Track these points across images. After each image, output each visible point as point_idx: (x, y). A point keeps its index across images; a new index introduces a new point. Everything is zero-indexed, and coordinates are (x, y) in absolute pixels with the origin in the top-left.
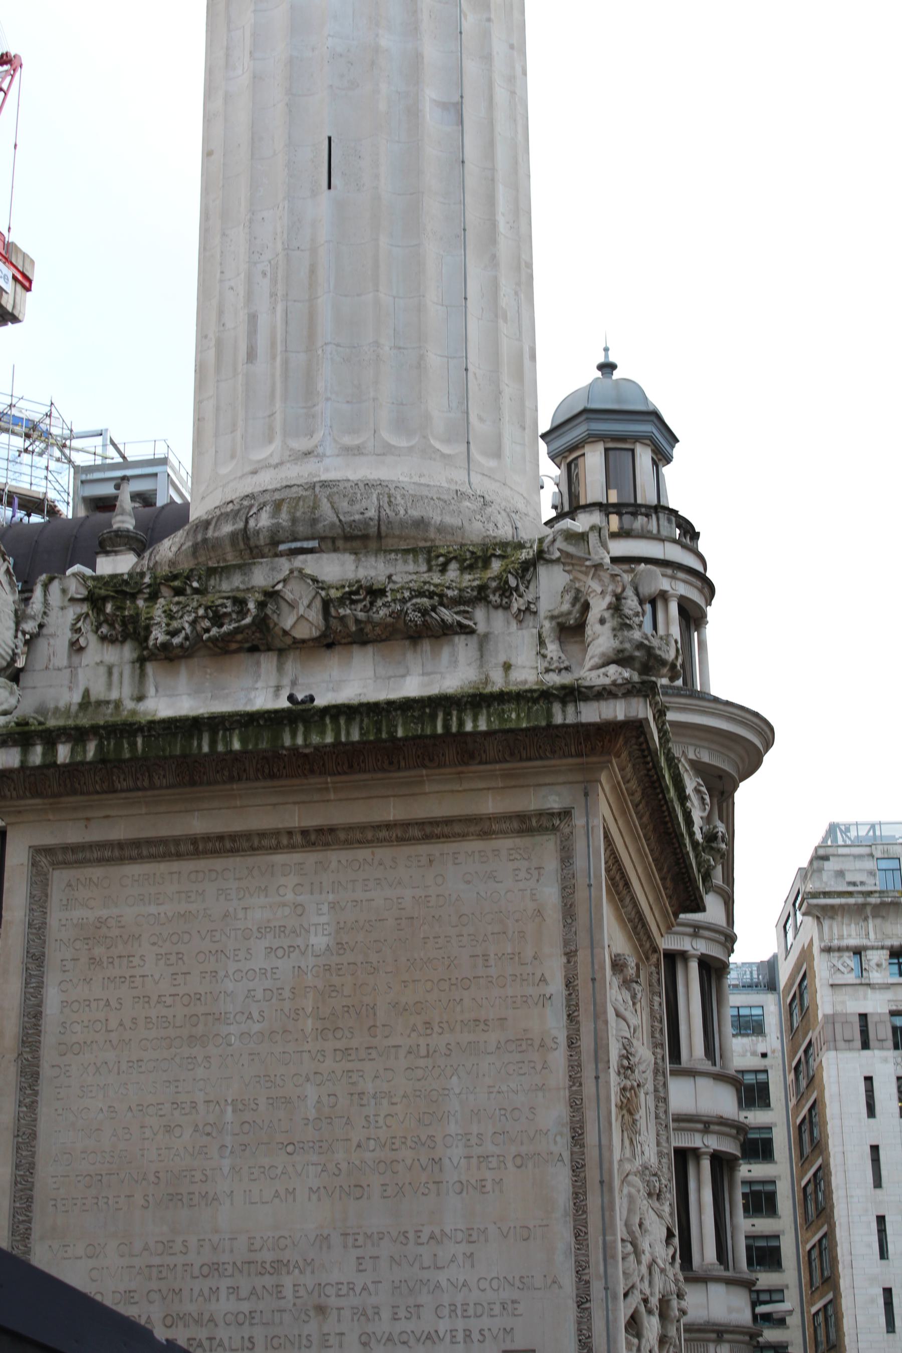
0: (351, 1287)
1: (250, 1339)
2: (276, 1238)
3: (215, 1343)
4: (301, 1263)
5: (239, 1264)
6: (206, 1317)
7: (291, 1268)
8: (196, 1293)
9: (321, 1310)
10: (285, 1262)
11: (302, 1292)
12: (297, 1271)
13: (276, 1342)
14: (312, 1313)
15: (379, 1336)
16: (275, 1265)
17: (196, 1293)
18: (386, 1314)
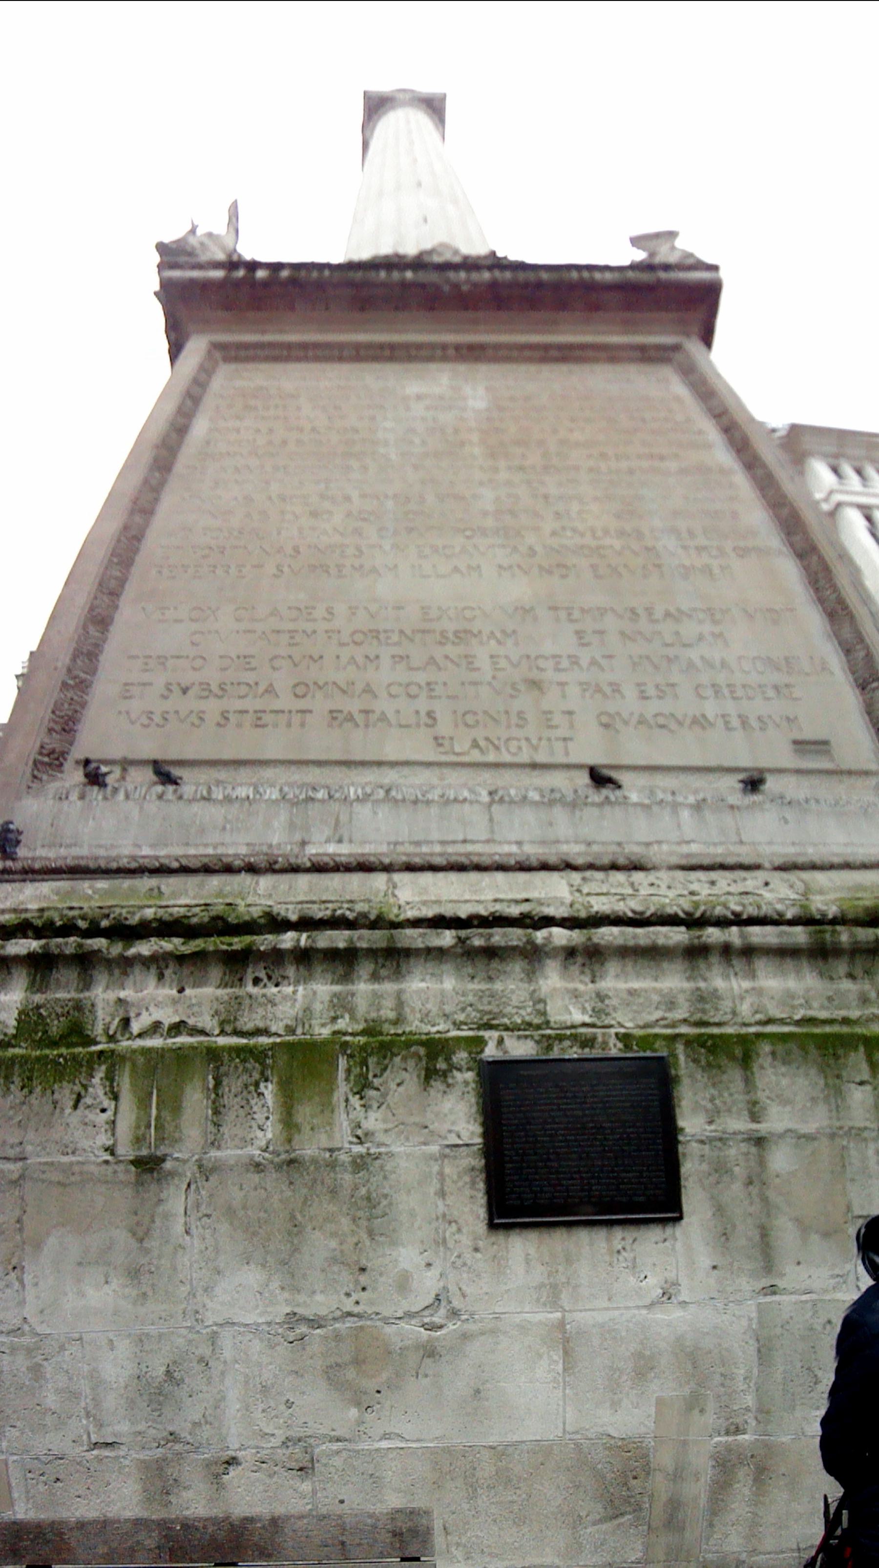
0: (574, 661)
1: (430, 714)
3: (373, 717)
4: (498, 635)
5: (408, 632)
6: (359, 686)
7: (485, 639)
8: (344, 660)
9: (535, 685)
10: (475, 631)
11: (503, 663)
13: (470, 719)
14: (522, 687)
15: (625, 715)
16: (462, 635)
17: (344, 660)
18: (630, 692)
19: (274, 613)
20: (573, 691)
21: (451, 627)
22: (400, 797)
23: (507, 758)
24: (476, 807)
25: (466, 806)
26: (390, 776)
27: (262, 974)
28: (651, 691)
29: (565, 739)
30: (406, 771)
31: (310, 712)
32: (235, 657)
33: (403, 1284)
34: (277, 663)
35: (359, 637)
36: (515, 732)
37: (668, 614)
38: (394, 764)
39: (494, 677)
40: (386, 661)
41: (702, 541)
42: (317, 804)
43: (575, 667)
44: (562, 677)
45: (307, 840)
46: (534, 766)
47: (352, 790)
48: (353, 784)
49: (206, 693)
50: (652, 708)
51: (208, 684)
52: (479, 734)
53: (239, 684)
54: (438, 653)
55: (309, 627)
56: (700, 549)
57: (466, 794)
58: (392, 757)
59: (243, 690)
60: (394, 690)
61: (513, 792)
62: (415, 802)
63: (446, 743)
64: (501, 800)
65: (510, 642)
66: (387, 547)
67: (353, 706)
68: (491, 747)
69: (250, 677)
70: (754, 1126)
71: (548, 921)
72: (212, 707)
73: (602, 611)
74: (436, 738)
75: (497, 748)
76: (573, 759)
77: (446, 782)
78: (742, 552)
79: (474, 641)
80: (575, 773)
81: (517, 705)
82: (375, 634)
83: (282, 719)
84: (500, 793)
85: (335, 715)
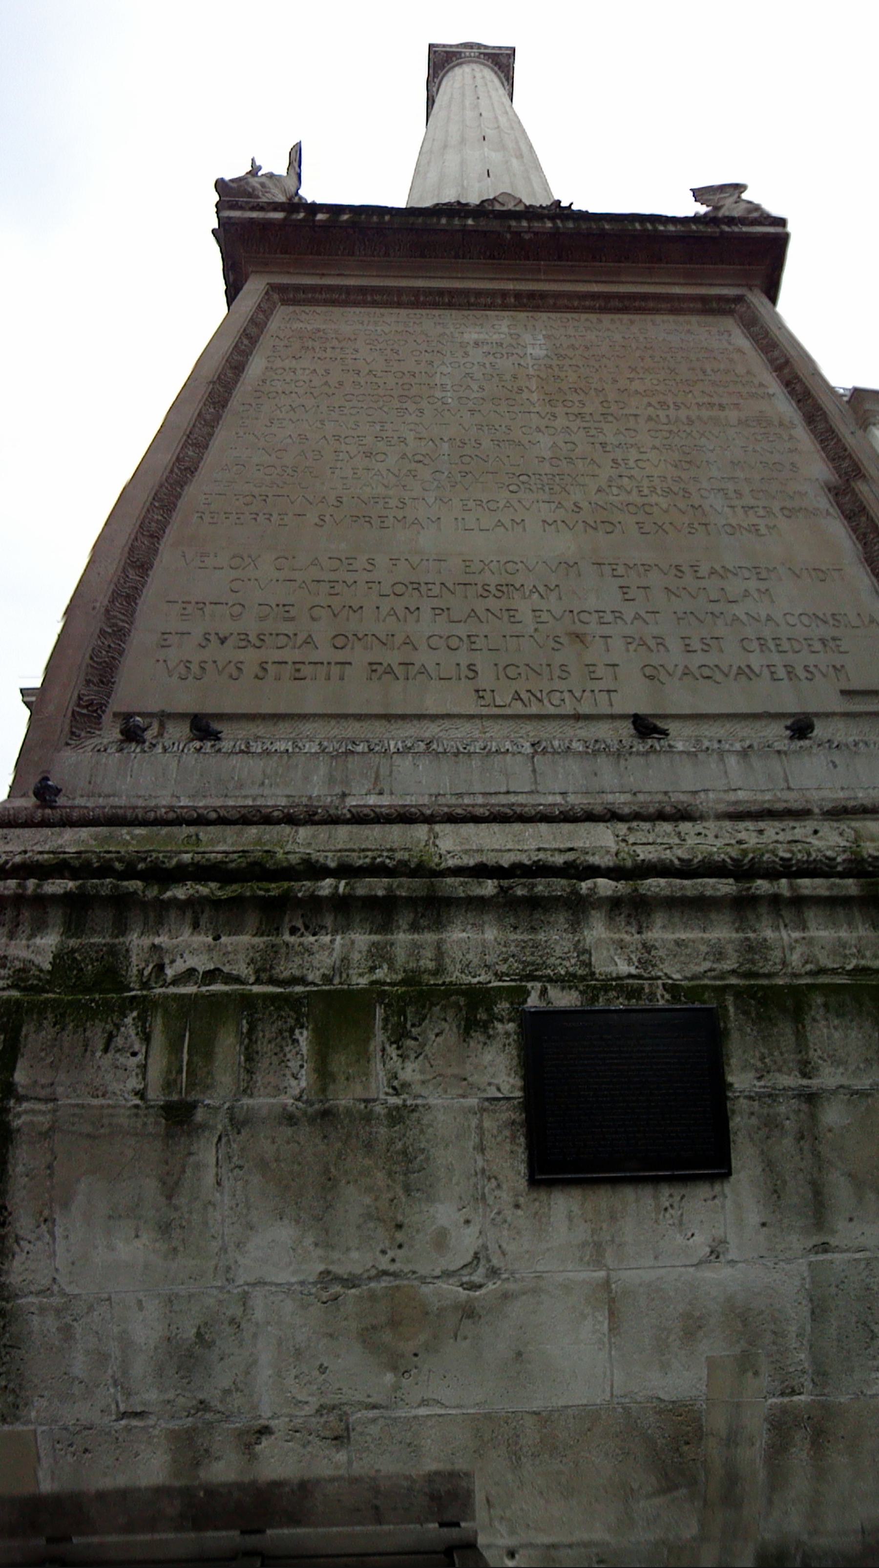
0: (618, 615)
1: (471, 667)
2: (502, 563)
3: (413, 670)
4: (541, 589)
5: (450, 585)
6: (399, 639)
7: (527, 593)
8: (384, 610)
9: (579, 637)
10: (518, 586)
11: (545, 617)
12: (536, 595)
13: (511, 672)
15: (670, 668)
16: (504, 589)
17: (384, 610)
18: (675, 645)
19: (315, 562)
20: (617, 644)
21: (493, 581)
22: (441, 749)
23: (552, 710)
24: (519, 758)
25: (509, 757)
26: (431, 730)
27: (299, 924)
28: (696, 645)
29: (608, 691)
30: (447, 724)
31: (350, 663)
32: (274, 606)
33: (441, 1241)
34: (317, 612)
35: (399, 589)
36: (558, 684)
37: (713, 572)
38: (434, 717)
39: (536, 630)
40: (426, 614)
41: (749, 501)
42: (356, 757)
43: (619, 620)
44: (606, 630)
45: (347, 792)
46: (577, 717)
47: (392, 743)
48: (393, 739)
49: (243, 644)
50: (698, 659)
51: (247, 635)
52: (521, 686)
53: (277, 635)
54: (480, 606)
55: (350, 578)
56: (747, 508)
57: (508, 746)
58: (433, 711)
59: (282, 640)
60: (434, 642)
61: (556, 743)
62: (457, 754)
63: (487, 695)
64: (544, 751)
65: (553, 597)
66: (431, 501)
67: (392, 658)
68: (532, 698)
69: (287, 628)
70: (805, 1082)
71: (594, 871)
72: (250, 657)
73: (647, 567)
74: (477, 691)
75: (540, 701)
76: (617, 710)
77: (488, 735)
78: (790, 513)
79: (517, 595)
80: (618, 724)
81: (559, 658)
82: (417, 586)
83: (322, 670)
84: (544, 744)
85: (374, 667)
